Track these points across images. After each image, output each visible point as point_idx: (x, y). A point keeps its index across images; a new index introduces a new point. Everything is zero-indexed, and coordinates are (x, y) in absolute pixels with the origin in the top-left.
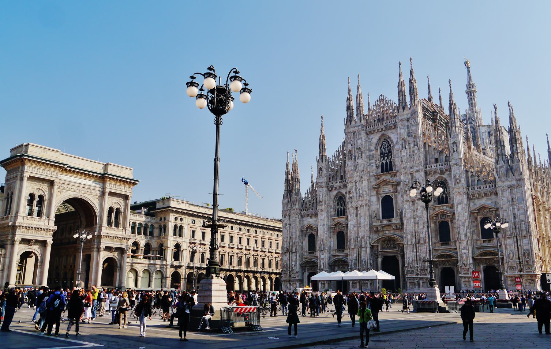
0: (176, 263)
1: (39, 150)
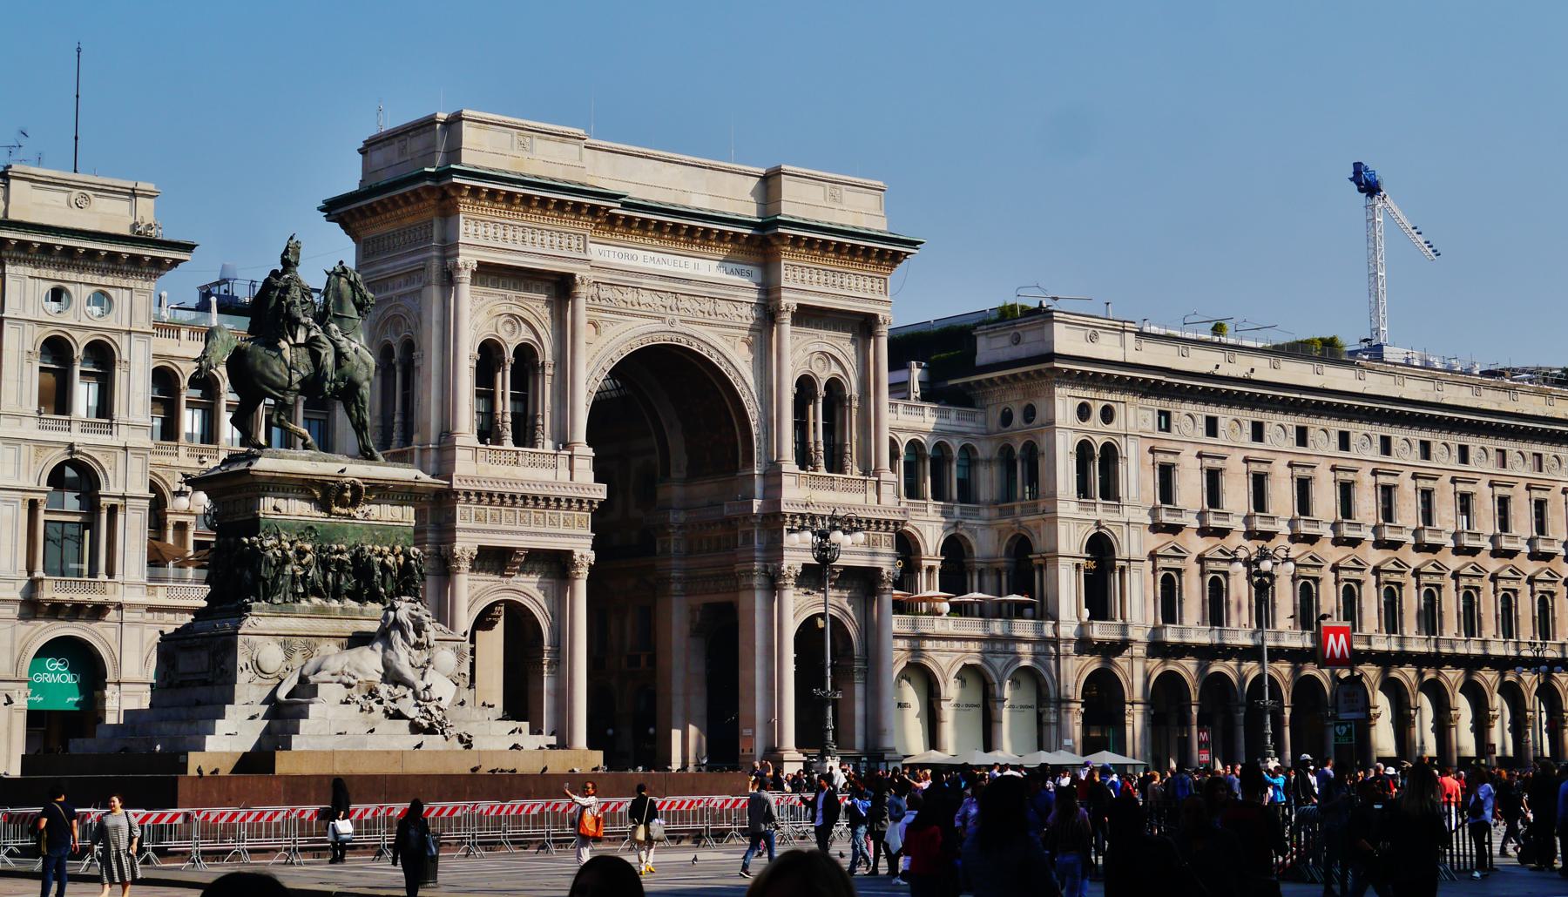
0: (1099, 631)
1: (503, 138)
